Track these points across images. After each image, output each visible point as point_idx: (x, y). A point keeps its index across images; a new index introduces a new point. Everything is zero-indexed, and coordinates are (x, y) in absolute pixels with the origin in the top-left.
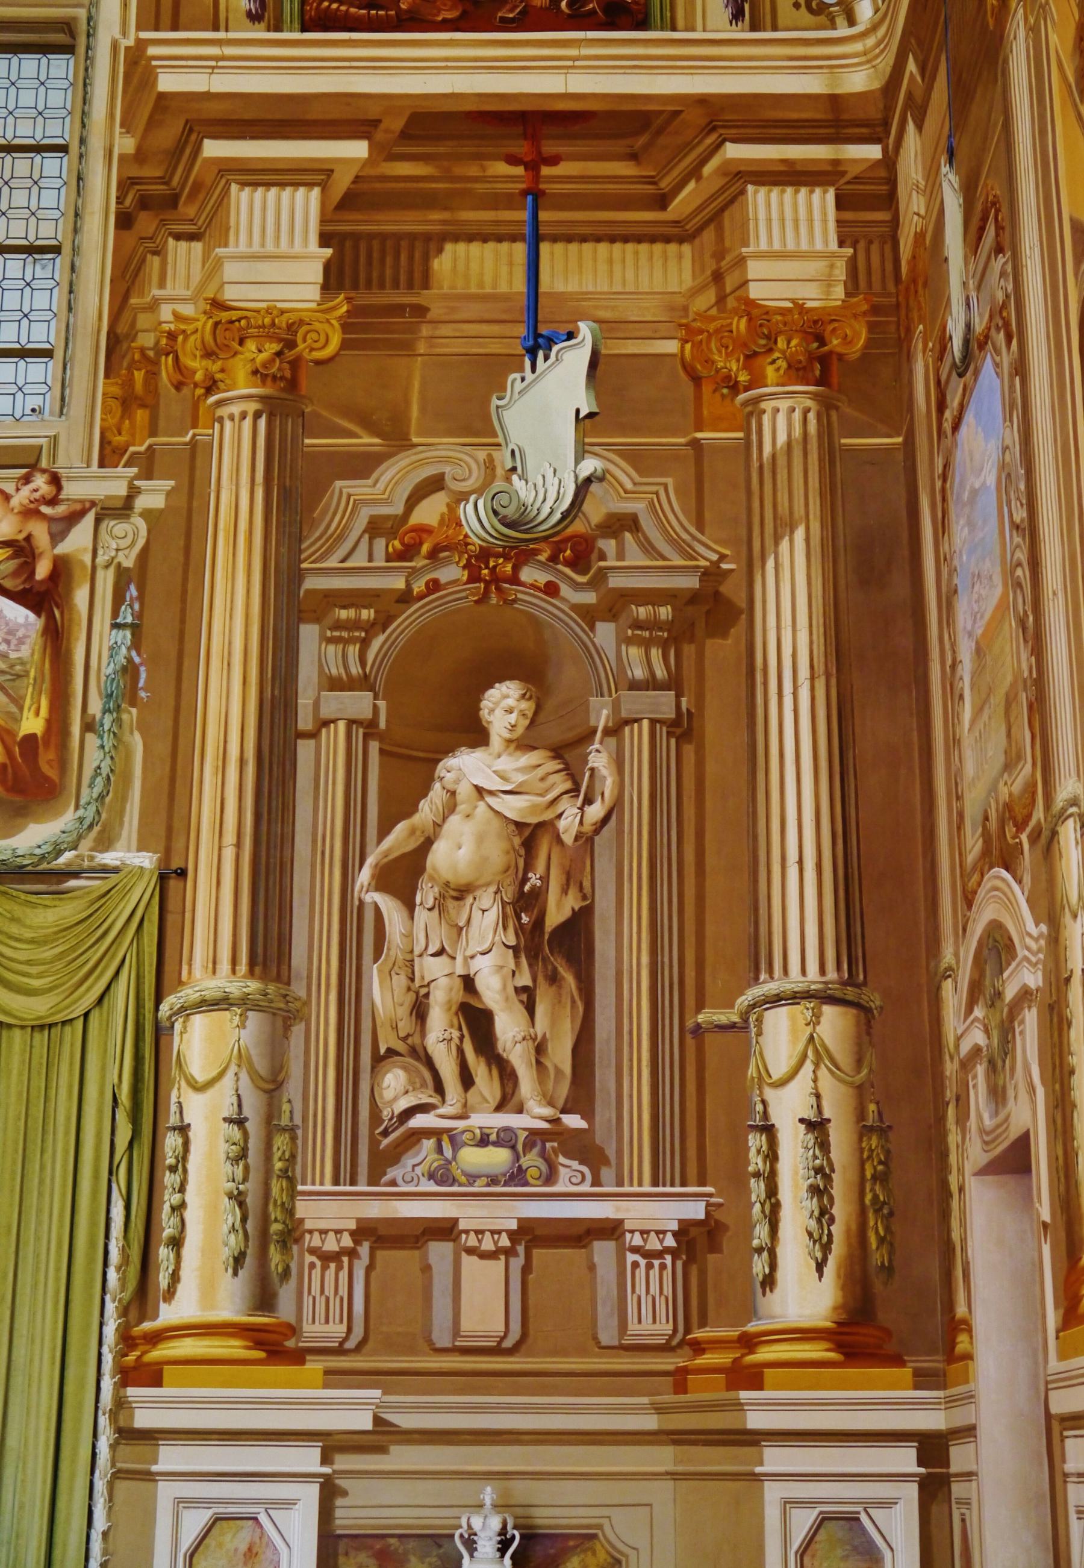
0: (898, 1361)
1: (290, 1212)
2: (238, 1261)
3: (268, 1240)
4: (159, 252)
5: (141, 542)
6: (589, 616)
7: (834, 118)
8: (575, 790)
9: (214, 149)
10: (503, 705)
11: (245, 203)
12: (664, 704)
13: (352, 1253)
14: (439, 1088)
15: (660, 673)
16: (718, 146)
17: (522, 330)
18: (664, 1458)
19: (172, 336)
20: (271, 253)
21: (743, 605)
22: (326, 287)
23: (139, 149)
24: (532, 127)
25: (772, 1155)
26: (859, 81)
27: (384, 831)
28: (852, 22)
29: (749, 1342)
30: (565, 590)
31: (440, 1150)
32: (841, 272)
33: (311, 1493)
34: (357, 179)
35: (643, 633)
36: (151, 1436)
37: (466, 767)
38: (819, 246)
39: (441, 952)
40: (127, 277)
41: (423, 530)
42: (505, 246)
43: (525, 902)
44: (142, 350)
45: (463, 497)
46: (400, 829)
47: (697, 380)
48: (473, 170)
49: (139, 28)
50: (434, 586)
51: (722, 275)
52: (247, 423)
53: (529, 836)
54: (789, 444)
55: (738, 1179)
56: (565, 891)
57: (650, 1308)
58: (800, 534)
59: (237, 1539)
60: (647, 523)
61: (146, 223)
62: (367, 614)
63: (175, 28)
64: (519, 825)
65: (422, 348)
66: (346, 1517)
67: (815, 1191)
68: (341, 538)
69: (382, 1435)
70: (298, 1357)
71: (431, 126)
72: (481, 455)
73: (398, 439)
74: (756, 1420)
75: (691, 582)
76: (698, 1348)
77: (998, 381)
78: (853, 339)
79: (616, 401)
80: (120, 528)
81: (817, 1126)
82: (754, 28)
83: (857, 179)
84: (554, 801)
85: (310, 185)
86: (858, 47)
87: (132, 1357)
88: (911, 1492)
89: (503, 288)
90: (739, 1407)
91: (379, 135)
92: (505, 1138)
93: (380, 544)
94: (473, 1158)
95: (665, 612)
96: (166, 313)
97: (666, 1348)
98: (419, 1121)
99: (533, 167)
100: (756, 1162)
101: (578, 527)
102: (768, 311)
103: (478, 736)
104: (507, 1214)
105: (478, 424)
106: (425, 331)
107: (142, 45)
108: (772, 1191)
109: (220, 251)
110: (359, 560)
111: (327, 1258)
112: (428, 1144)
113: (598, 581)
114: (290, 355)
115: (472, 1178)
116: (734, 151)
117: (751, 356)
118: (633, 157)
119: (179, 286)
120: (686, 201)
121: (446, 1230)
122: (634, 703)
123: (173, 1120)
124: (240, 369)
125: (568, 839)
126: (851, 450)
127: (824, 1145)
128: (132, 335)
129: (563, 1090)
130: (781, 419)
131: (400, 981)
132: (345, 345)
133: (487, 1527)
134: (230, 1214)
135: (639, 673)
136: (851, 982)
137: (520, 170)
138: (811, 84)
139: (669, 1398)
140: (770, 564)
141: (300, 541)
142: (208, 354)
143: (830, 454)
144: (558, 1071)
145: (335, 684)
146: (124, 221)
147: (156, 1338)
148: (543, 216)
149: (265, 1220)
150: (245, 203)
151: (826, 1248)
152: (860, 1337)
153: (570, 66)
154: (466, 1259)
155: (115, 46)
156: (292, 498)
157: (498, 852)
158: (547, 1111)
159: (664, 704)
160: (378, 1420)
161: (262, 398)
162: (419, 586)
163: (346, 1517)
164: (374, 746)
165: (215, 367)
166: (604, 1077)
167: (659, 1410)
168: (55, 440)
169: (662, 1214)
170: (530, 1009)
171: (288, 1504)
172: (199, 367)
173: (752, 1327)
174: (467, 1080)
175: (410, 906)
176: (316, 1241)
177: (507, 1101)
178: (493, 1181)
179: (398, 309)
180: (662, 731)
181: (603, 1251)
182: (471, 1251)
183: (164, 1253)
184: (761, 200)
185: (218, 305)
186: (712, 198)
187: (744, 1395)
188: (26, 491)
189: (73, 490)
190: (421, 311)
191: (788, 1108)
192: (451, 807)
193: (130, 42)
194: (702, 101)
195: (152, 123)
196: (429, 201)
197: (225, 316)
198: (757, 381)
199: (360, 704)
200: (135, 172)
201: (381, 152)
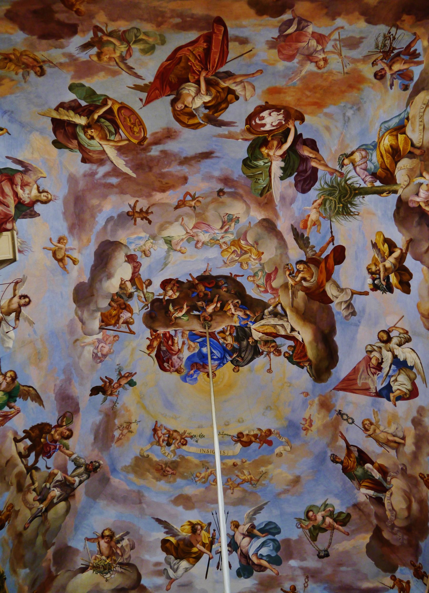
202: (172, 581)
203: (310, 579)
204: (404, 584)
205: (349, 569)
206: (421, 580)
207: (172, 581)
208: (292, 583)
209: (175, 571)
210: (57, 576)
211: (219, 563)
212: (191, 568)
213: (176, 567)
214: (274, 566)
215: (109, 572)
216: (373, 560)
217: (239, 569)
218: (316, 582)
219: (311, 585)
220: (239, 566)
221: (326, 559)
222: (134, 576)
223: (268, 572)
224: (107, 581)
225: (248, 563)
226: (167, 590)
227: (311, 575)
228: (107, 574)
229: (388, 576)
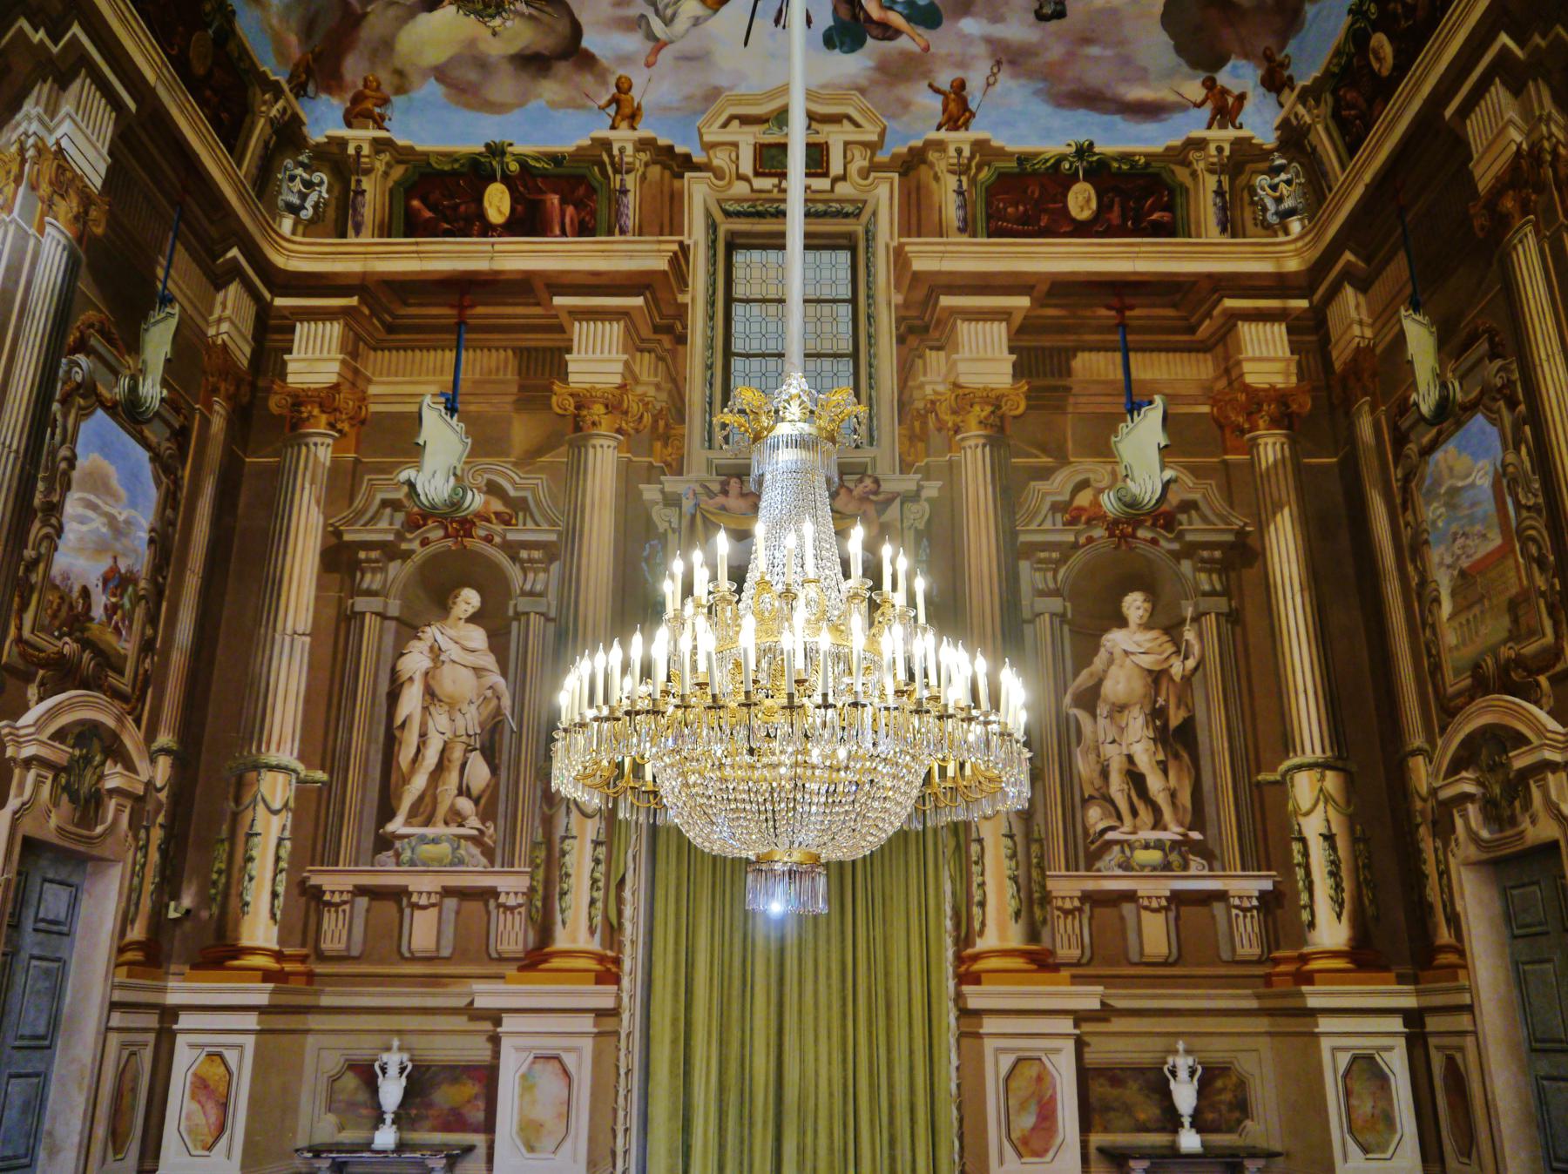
0: (1386, 969)
1: (1044, 887)
2: (1017, 914)
3: (1034, 904)
4: (921, 356)
5: (927, 516)
6: (1177, 556)
7: (1279, 285)
8: (1178, 652)
9: (946, 301)
10: (1135, 605)
11: (965, 329)
12: (1222, 604)
13: (1080, 910)
14: (1120, 818)
15: (1218, 587)
16: (1219, 300)
17: (1123, 400)
18: (1263, 1024)
19: (933, 403)
20: (983, 357)
21: (1259, 549)
22: (1014, 376)
23: (905, 300)
24: (1120, 290)
25: (1306, 854)
26: (1293, 265)
27: (1076, 674)
28: (1287, 233)
29: (1305, 959)
30: (1163, 543)
31: (1123, 851)
32: (1293, 369)
33: (1070, 1045)
34: (1026, 318)
35: (1208, 566)
36: (979, 1013)
37: (1116, 639)
38: (1280, 354)
39: (1113, 742)
40: (905, 371)
41: (1081, 509)
42: (1110, 354)
43: (1157, 714)
44: (918, 411)
45: (1101, 491)
46: (1085, 673)
47: (1221, 427)
48: (1088, 313)
49: (900, 235)
50: (1090, 540)
51: (1230, 368)
52: (979, 450)
53: (1157, 677)
54: (1275, 461)
55: (1287, 867)
56: (1178, 707)
57: (1247, 938)
58: (1286, 511)
59: (1031, 1071)
60: (1202, 504)
61: (913, 341)
62: (1055, 555)
63: (919, 236)
64: (1150, 671)
65: (1070, 409)
66: (1091, 1057)
67: (1332, 874)
68: (1036, 513)
69: (1106, 1013)
70: (1056, 968)
71: (1063, 289)
72: (1109, 468)
73: (1063, 461)
74: (1312, 1002)
75: (1229, 538)
76: (1277, 962)
78: (1304, 404)
79: (1181, 438)
80: (914, 507)
81: (1329, 838)
82: (1233, 236)
83: (1297, 318)
84: (1168, 658)
85: (1001, 321)
86: (1292, 247)
87: (963, 969)
88: (1402, 1042)
89: (1111, 377)
90: (1302, 995)
91: (1035, 294)
92: (1159, 845)
93: (1058, 516)
94: (1142, 856)
95: (1217, 554)
96: (928, 390)
97: (1259, 962)
98: (1110, 836)
99: (1121, 311)
100: (1298, 858)
101: (1165, 507)
102: (1257, 390)
103: (1122, 622)
104: (1165, 887)
105: (1103, 450)
106: (1071, 400)
107: (901, 246)
108: (1308, 874)
109: (955, 356)
110: (1048, 525)
111: (1067, 912)
112: (1117, 848)
113: (1180, 536)
114: (999, 413)
115: (1142, 867)
116: (1229, 303)
117: (1249, 415)
118: (1174, 306)
119: (934, 376)
120: (1206, 329)
121: (1131, 896)
122: (1206, 604)
123: (974, 835)
124: (972, 421)
125: (1177, 678)
126: (1310, 466)
127: (1333, 847)
128: (912, 401)
129: (1188, 819)
130: (1270, 448)
131: (1092, 757)
132: (1028, 407)
133: (1183, 1063)
134: (1010, 889)
135: (1207, 587)
136: (1340, 757)
137: (1113, 313)
138: (1266, 267)
139: (1262, 990)
140: (1272, 527)
141: (1014, 513)
142: (954, 412)
143: (1299, 469)
144: (1184, 808)
145: (1042, 594)
146: (901, 340)
147: (977, 957)
148: (1129, 338)
149: (1030, 893)
150: (965, 329)
151: (1341, 905)
152: (1365, 955)
153: (1136, 256)
154: (1145, 915)
155: (887, 246)
156: (1008, 492)
157: (1139, 686)
158: (1181, 830)
159: (1222, 604)
160: (1103, 1003)
161: (985, 437)
162: (1082, 540)
163: (1091, 1057)
164: (1066, 628)
165: (958, 419)
166: (1210, 810)
167: (1258, 997)
168: (874, 459)
169: (1249, 886)
170: (1165, 772)
171: (1057, 1051)
172: (950, 420)
173: (1306, 950)
174: (1135, 813)
175: (1094, 716)
176: (1060, 903)
177: (1158, 824)
178: (1154, 869)
179: (1055, 389)
180: (1223, 620)
181: (1218, 908)
182: (1146, 908)
183: (976, 910)
184: (1247, 331)
185: (956, 385)
186: (1220, 328)
187: (1305, 988)
188: (861, 486)
189: (886, 487)
190: (1069, 389)
191: (1313, 827)
192: (1111, 662)
193: (895, 243)
195: (911, 287)
196: (1063, 329)
197: (960, 392)
198: (1254, 428)
199: (1056, 604)
200: (903, 313)
201: (1038, 303)
202: (659, 45)
203: (1005, 67)
204: (1230, 100)
205: (1108, 53)
206: (1274, 95)
207: (659, 45)
208: (959, 74)
209: (668, 22)
210: (365, 15)
211: (780, 11)
212: (706, 19)
213: (669, 12)
214: (921, 30)
215: (499, 14)
216: (1172, 37)
217: (830, 29)
218: (1015, 76)
219: (1005, 80)
220: (831, 23)
221: (1053, 25)
222: (563, 27)
223: (903, 43)
224: (495, 34)
225: (855, 17)
226: (648, 65)
227: (1008, 57)
228: (493, 17)
229: (1194, 78)
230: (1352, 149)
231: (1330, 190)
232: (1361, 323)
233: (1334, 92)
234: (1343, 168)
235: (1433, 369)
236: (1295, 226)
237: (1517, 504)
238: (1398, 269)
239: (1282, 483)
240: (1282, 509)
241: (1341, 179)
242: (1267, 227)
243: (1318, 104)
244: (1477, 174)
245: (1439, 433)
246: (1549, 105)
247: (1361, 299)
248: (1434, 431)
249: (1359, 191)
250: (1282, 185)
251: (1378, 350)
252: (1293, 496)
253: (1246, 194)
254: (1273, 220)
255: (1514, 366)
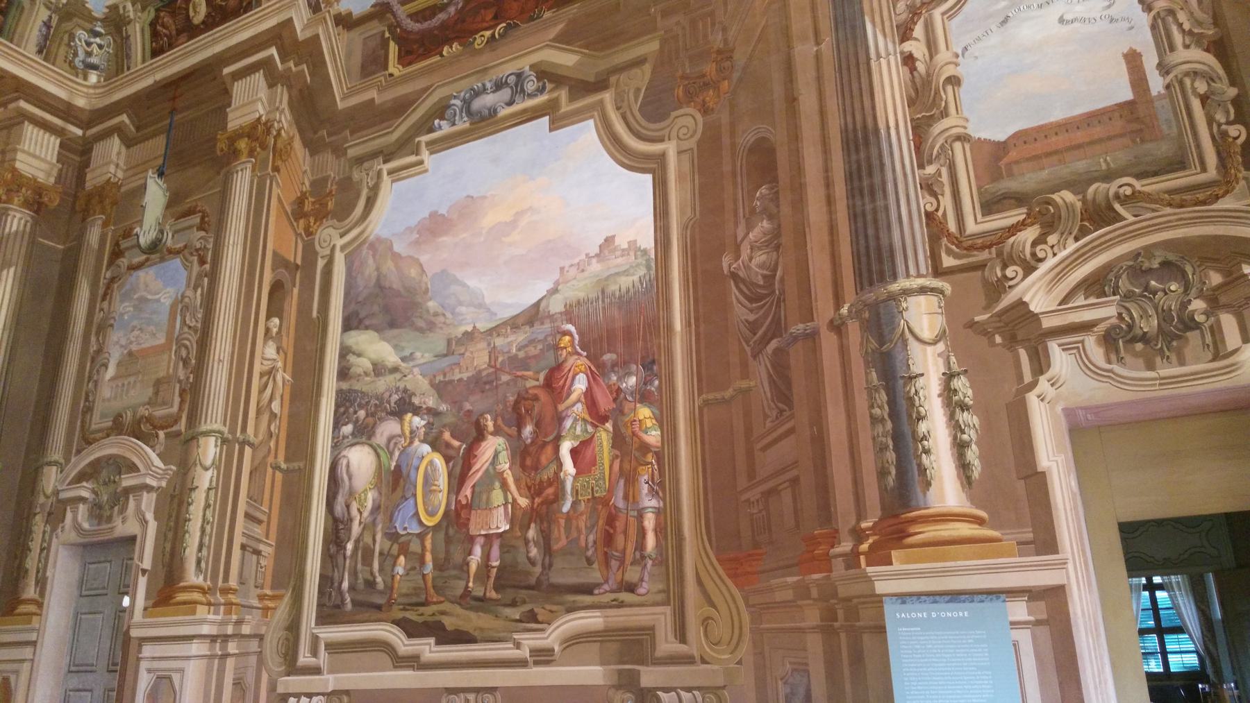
7: (66, 111)
26: (80, 102)
28: (85, 78)
32: (55, 173)
54: (17, 232)
58: (12, 270)
77: (185, 273)
86: (85, 90)
102: (21, 175)
116: (23, 104)
117: (9, 191)
126: (41, 243)
130: (16, 221)
138: (62, 94)
143: (33, 242)
184: (29, 130)
194: (15, 77)
198: (9, 201)
230: (155, 53)
231: (129, 69)
232: (117, 166)
233: (157, 10)
234: (144, 61)
235: (157, 219)
236: (93, 78)
237: (184, 322)
238: (158, 145)
239: (17, 246)
240: (10, 266)
241: (140, 67)
242: (71, 65)
243: (143, 9)
244: (230, 116)
245: (147, 260)
246: (285, 105)
247: (124, 149)
248: (144, 257)
249: (148, 82)
250: (95, 46)
251: (123, 189)
252: (21, 262)
253: (66, 37)
254: (78, 62)
255: (211, 240)
